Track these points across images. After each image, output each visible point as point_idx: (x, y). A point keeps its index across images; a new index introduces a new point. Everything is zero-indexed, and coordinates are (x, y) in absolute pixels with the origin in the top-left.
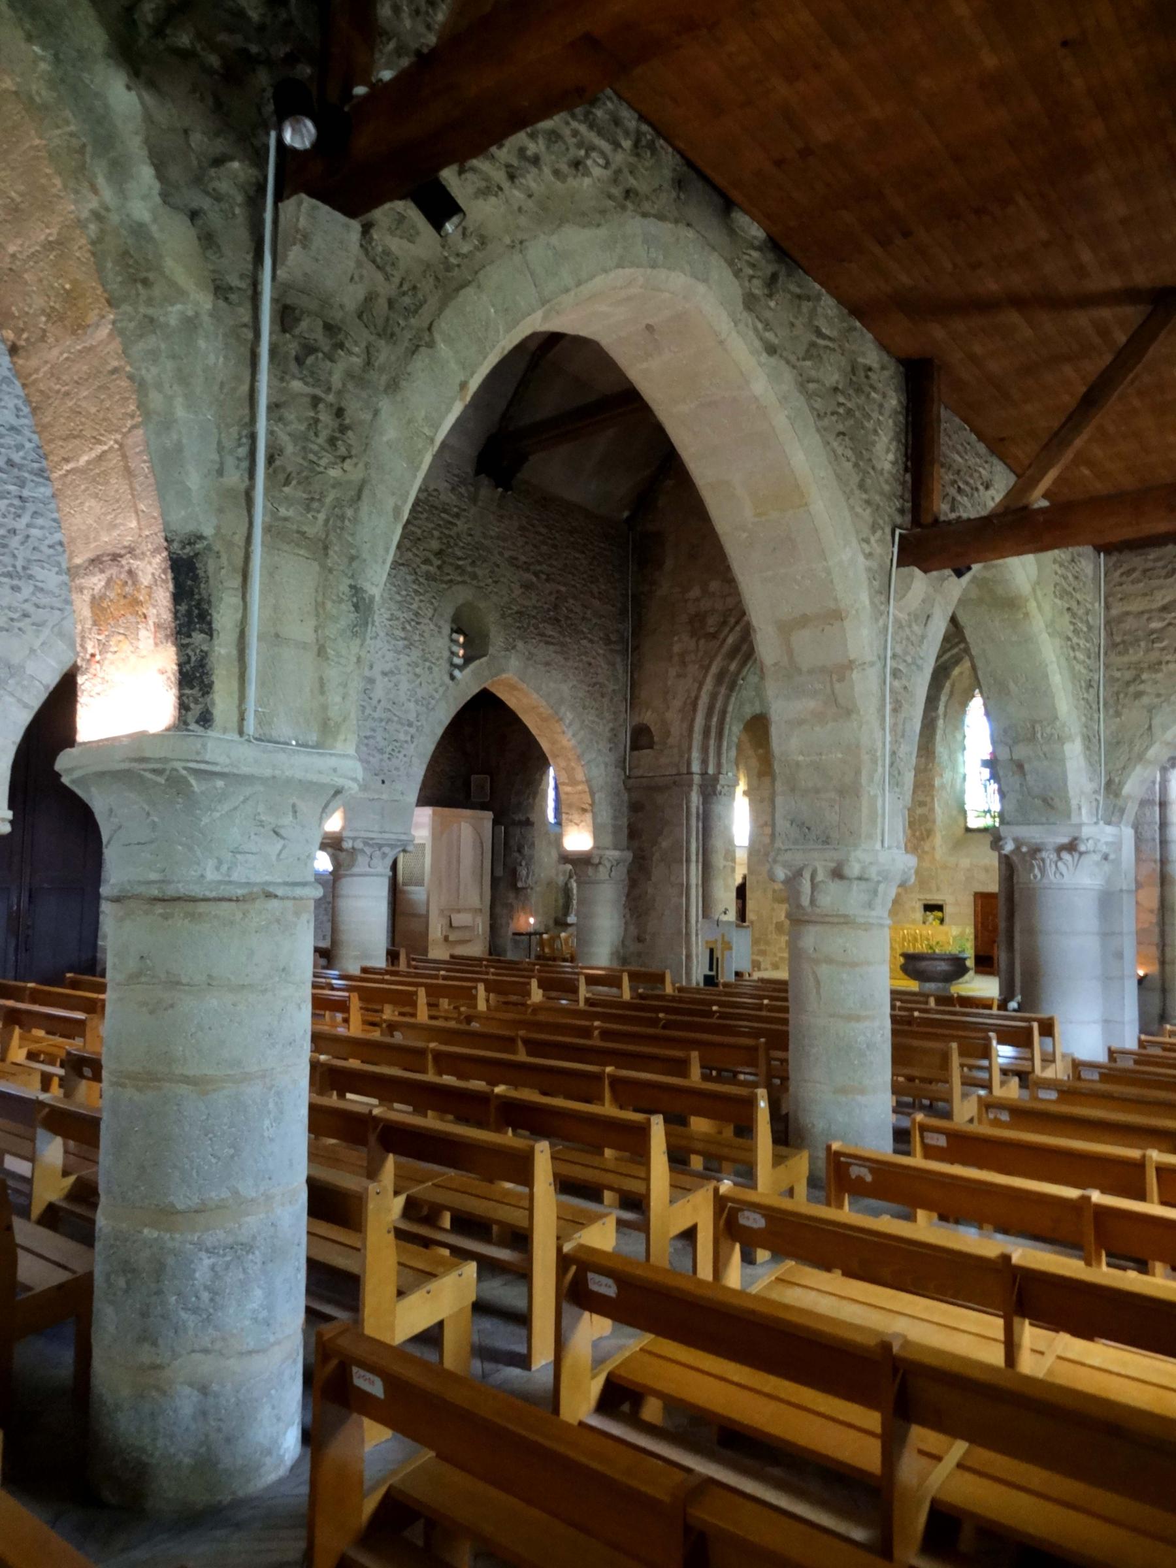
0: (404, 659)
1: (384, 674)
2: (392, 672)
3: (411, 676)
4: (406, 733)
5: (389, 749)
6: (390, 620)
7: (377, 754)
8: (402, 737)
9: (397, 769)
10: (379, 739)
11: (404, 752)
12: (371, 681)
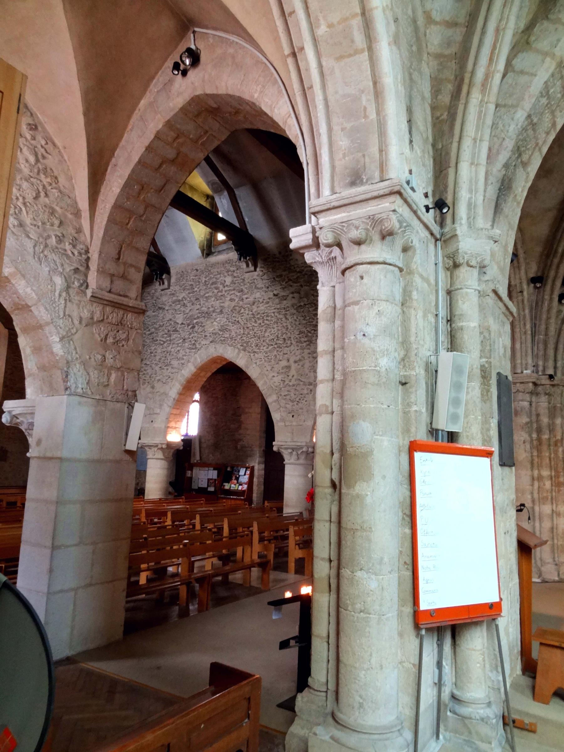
0: (306, 351)
1: (295, 362)
2: (300, 360)
3: (311, 359)
4: (307, 389)
5: (297, 399)
6: (299, 334)
7: (290, 403)
8: (305, 391)
9: (302, 409)
10: (292, 395)
11: (305, 399)
12: (289, 367)
